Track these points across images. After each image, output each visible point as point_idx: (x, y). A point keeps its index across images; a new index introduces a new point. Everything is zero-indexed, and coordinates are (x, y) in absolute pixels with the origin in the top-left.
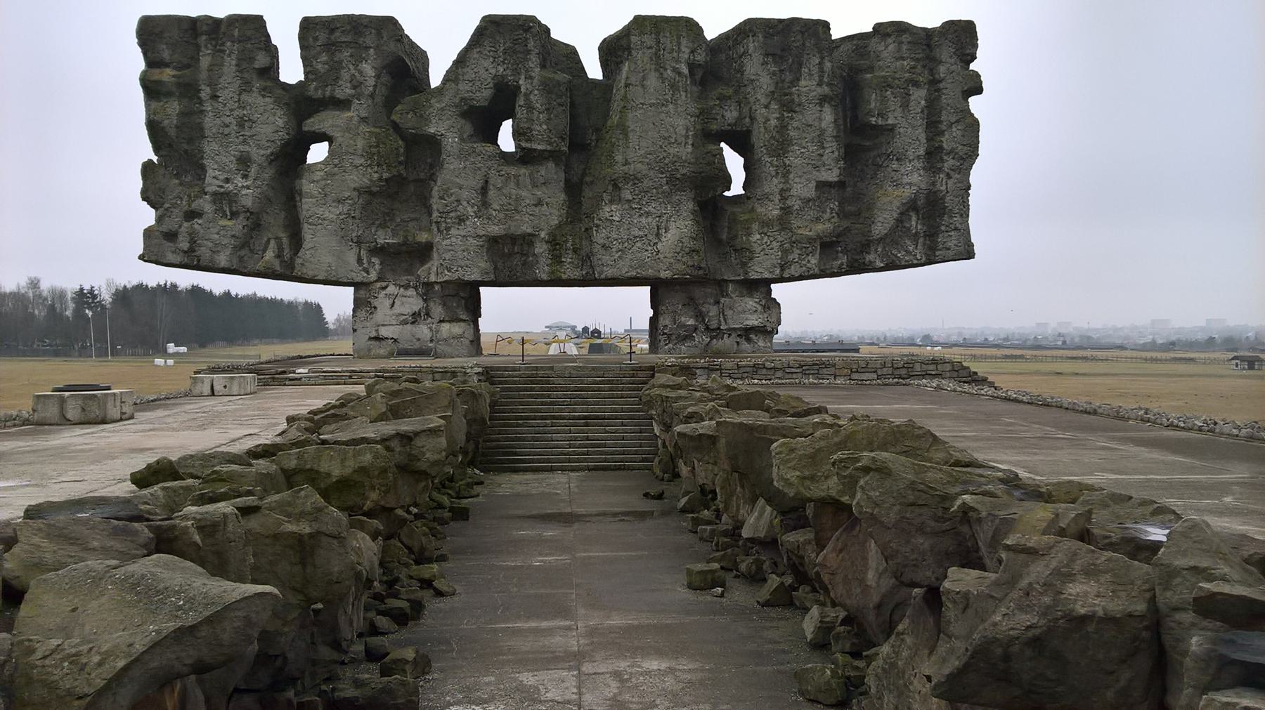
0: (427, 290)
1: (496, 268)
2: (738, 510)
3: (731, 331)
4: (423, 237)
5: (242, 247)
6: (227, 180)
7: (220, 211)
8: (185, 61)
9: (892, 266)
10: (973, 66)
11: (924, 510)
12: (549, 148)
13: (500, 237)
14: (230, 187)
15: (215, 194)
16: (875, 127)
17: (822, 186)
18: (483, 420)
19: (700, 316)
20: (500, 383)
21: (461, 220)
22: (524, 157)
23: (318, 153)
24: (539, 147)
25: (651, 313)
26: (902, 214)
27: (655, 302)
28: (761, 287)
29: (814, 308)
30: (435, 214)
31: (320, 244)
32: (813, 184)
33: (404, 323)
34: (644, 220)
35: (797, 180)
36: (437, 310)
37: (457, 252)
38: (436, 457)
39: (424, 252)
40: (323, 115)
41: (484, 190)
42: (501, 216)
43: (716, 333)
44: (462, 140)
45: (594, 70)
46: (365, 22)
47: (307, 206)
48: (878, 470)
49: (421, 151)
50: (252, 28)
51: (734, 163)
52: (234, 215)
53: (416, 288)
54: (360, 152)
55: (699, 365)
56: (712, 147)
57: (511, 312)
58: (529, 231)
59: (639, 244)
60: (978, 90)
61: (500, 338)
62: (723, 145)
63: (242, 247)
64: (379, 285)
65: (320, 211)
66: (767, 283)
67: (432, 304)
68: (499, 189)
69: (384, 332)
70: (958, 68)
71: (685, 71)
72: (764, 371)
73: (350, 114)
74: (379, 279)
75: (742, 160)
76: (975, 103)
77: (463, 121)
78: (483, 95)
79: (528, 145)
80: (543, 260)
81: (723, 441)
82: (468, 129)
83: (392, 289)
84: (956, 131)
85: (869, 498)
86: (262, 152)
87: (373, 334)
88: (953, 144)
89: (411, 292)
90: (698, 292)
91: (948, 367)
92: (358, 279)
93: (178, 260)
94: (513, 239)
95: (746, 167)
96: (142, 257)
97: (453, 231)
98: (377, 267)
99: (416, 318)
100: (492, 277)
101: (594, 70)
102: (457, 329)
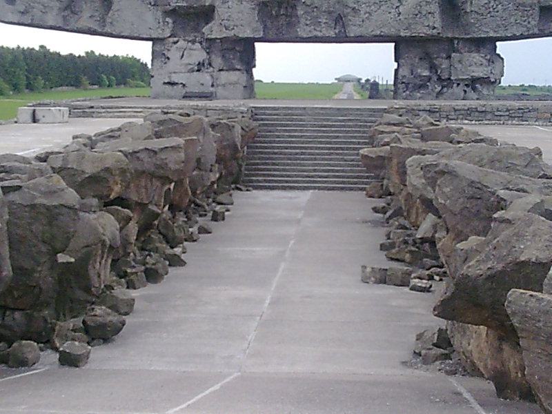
1: (265, 27)
2: (417, 217)
5: (66, 9)
11: (479, 201)
18: (236, 146)
19: (433, 68)
20: (262, 120)
28: (486, 44)
33: (192, 71)
36: (218, 61)
38: (177, 167)
48: (449, 173)
53: (201, 43)
55: (421, 108)
57: (278, 63)
61: (278, 89)
63: (66, 9)
64: (171, 40)
67: (213, 56)
69: (175, 79)
72: (477, 113)
80: (303, 21)
81: (395, 161)
83: (182, 43)
85: (443, 193)
90: (433, 49)
98: (170, 25)
99: (200, 67)
102: (233, 76)
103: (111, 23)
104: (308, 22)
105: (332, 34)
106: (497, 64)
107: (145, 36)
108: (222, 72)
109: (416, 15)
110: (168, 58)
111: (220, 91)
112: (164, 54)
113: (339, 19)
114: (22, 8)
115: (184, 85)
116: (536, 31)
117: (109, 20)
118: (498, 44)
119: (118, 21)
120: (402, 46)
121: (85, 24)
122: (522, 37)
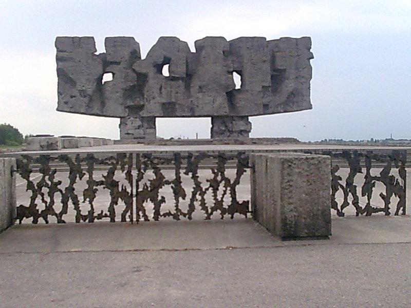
3: (235, 132)
9: (285, 112)
10: (311, 51)
14: (84, 88)
15: (79, 90)
17: (263, 87)
19: (226, 127)
22: (171, 78)
23: (108, 77)
25: (211, 126)
27: (212, 123)
29: (263, 126)
30: (145, 96)
31: (111, 105)
32: (261, 87)
33: (136, 129)
36: (146, 125)
37: (152, 106)
39: (141, 107)
41: (161, 89)
42: (166, 96)
43: (231, 132)
44: (154, 74)
45: (193, 50)
47: (107, 94)
49: (142, 78)
50: (91, 40)
51: (237, 78)
52: (85, 97)
56: (230, 76)
57: (166, 127)
60: (313, 58)
62: (235, 74)
64: (128, 117)
66: (248, 116)
68: (165, 88)
69: (129, 132)
70: (306, 50)
71: (222, 53)
73: (119, 66)
75: (239, 77)
76: (311, 60)
77: (154, 68)
78: (161, 61)
80: (178, 111)
82: (156, 70)
83: (132, 118)
87: (126, 132)
88: (306, 74)
89: (138, 119)
90: (225, 119)
91: (293, 140)
92: (122, 116)
94: (169, 103)
95: (241, 80)
96: (57, 110)
97: (151, 101)
98: (128, 112)
99: (139, 127)
100: (162, 115)
101: (193, 50)
106: (249, 125)
107: (118, 116)
110: (127, 124)
111: (147, 137)
114: (71, 106)
115: (133, 134)
116: (262, 113)
117: (104, 110)
118: (250, 118)
120: (214, 119)
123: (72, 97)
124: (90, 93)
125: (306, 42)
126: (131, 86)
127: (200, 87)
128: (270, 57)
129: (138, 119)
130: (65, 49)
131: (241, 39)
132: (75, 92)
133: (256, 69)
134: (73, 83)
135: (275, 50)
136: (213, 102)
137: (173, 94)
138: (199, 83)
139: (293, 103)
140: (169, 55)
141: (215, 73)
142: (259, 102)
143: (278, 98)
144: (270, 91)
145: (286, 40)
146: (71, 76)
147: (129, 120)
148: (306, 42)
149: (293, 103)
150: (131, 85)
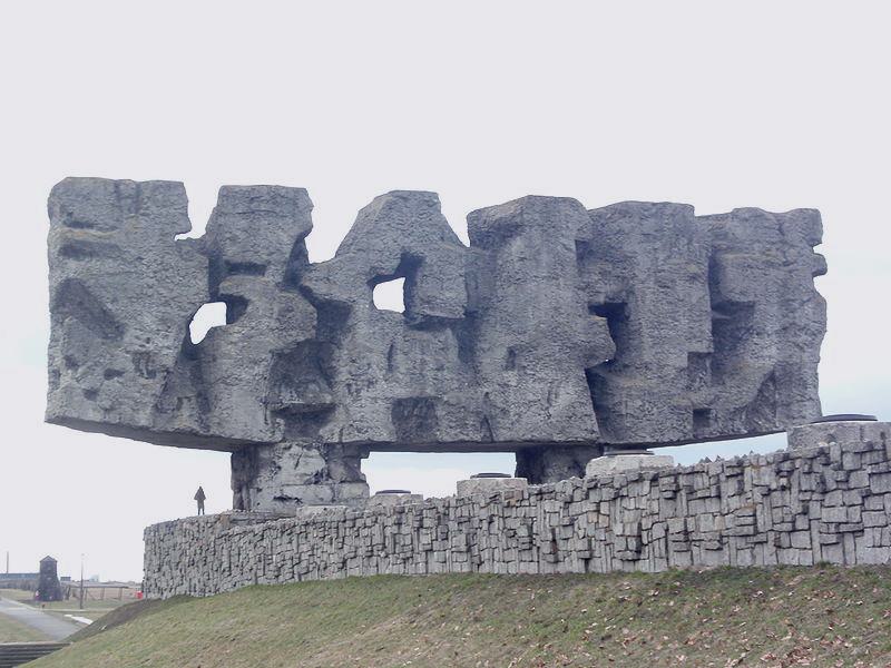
0: (328, 450)
4: (328, 399)
6: (148, 340)
7: (138, 369)
8: (112, 223)
10: (817, 249)
12: (450, 316)
13: (406, 400)
14: (150, 347)
15: (136, 353)
16: (733, 304)
17: (695, 357)
21: (371, 383)
24: (442, 315)
26: (763, 384)
32: (685, 356)
33: (308, 483)
34: (537, 386)
35: (672, 351)
36: (339, 471)
37: (367, 411)
39: (321, 414)
40: (238, 278)
42: (407, 379)
46: (283, 192)
49: (333, 316)
50: (172, 194)
52: (152, 374)
53: (318, 448)
54: (275, 316)
57: (385, 472)
58: (433, 394)
59: (533, 409)
60: (823, 272)
64: (283, 445)
65: (237, 372)
69: (288, 492)
71: (573, 247)
73: (265, 279)
74: (284, 440)
76: (818, 280)
79: (432, 313)
80: (445, 423)
83: (295, 449)
84: (809, 308)
86: (183, 314)
87: (278, 495)
90: (581, 456)
93: (96, 416)
94: (416, 402)
98: (282, 427)
99: (318, 478)
103: (219, 423)
104: (453, 425)
105: (478, 437)
108: (344, 485)
109: (570, 418)
110: (279, 468)
112: (274, 463)
113: (486, 422)
114: (107, 404)
119: (227, 422)
121: (188, 424)
122: (679, 443)
123: (110, 374)
124: (169, 362)
125: (808, 225)
126: (298, 344)
127: (511, 352)
128: (705, 268)
129: (314, 452)
130: (90, 214)
131: (623, 210)
132: (123, 361)
133: (670, 299)
134: (109, 326)
135: (723, 244)
136: (548, 400)
137: (430, 374)
138: (508, 338)
139: (774, 406)
140: (417, 248)
141: (556, 309)
142: (685, 402)
143: (734, 391)
144: (709, 370)
145: (753, 217)
146: (110, 306)
147: (287, 453)
148: (808, 225)
149: (774, 406)
150: (302, 339)
